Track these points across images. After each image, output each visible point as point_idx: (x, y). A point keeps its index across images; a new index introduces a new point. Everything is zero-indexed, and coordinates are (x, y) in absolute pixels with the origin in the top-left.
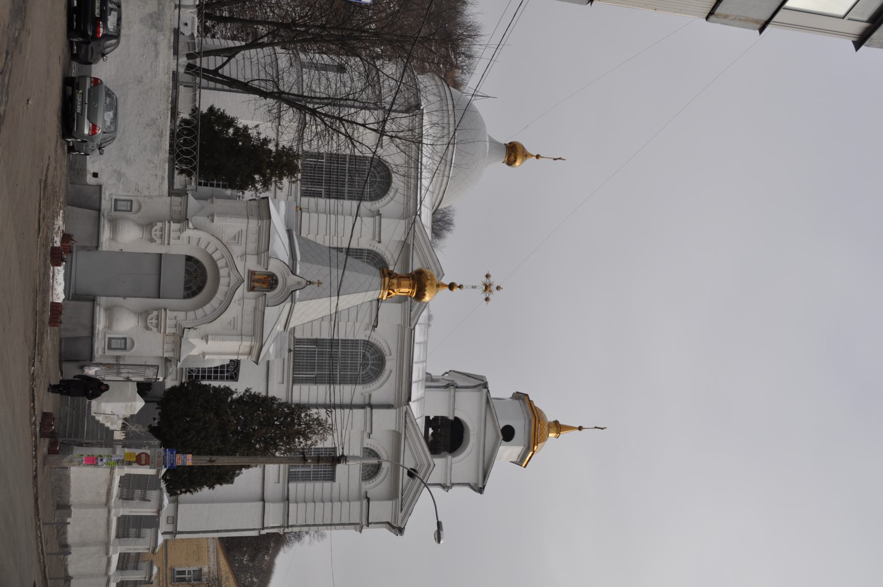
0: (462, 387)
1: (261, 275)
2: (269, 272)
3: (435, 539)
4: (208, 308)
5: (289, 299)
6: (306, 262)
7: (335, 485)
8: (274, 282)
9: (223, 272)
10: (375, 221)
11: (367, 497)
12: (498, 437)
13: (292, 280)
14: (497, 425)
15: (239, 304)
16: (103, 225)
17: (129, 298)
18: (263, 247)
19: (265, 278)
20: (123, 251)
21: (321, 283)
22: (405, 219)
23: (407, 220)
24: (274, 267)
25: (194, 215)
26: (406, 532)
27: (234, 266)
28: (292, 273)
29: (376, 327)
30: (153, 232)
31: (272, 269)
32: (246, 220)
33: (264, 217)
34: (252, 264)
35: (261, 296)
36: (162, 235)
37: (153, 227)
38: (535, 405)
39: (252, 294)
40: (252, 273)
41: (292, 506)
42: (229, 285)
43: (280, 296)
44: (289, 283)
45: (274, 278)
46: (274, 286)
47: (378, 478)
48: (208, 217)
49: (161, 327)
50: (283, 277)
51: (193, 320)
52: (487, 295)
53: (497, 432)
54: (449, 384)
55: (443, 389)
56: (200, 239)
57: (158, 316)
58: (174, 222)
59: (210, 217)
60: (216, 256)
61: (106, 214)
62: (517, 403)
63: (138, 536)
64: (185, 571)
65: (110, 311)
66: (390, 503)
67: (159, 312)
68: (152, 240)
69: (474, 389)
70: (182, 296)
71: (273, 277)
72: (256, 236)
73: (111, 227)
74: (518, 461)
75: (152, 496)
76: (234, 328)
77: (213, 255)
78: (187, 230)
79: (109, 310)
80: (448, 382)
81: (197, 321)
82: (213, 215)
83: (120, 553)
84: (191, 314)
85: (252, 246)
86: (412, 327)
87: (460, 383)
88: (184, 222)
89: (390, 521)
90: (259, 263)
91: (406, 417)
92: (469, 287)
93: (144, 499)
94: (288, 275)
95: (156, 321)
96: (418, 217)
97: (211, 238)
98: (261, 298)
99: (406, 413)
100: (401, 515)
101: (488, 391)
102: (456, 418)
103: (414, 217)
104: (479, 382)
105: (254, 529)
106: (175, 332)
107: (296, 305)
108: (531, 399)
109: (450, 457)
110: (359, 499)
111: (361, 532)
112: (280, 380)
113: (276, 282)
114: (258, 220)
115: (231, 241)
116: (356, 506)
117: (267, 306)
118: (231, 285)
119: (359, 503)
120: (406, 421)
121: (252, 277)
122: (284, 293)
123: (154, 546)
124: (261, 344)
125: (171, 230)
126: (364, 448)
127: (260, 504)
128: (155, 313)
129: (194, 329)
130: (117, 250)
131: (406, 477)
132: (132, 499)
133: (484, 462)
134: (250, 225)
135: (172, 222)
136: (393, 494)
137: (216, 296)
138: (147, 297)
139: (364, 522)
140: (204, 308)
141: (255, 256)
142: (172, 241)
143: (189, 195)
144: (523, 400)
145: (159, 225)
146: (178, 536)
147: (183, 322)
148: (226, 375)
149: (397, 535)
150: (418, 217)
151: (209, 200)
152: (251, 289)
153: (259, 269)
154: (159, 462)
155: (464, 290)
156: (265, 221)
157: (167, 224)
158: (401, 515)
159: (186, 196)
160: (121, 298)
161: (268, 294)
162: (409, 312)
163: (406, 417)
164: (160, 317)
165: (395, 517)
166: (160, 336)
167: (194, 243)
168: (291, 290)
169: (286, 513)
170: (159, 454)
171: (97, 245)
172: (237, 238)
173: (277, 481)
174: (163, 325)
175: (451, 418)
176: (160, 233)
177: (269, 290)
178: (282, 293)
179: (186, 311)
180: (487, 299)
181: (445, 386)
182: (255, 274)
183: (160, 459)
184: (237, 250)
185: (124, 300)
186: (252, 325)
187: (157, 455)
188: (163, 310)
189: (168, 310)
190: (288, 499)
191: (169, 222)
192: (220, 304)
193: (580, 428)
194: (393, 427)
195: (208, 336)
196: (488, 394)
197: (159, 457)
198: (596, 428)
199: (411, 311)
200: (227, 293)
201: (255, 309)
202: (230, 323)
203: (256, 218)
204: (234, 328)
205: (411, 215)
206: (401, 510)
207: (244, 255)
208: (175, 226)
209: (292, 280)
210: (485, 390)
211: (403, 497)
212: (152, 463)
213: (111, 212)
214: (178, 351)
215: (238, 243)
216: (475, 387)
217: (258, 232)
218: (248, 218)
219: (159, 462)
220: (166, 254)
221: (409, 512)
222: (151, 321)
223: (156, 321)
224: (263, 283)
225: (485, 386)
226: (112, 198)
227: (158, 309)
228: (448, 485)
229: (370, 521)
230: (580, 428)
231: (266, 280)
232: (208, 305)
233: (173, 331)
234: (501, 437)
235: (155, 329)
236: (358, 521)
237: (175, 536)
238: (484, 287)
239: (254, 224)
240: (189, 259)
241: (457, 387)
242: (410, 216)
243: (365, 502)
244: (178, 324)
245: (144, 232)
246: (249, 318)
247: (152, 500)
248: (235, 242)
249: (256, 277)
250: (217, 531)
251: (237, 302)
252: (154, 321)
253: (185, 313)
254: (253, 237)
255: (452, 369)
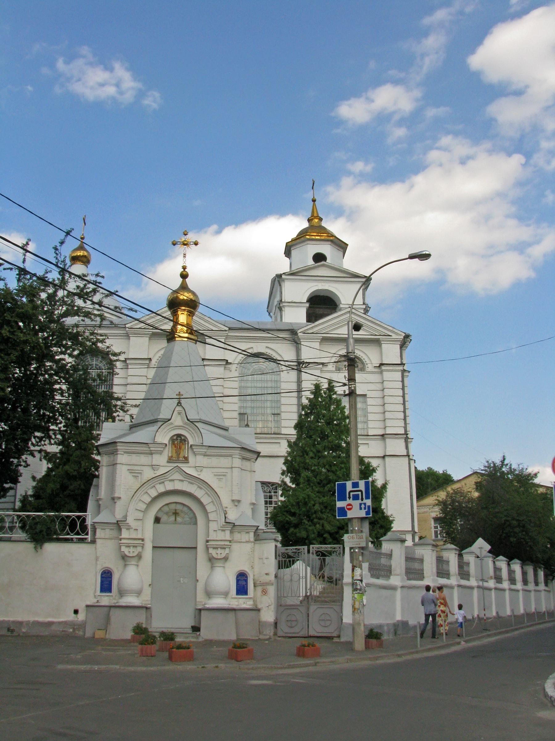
0: (281, 296)
1: (172, 452)
2: (169, 443)
3: (427, 259)
4: (205, 500)
5: (196, 424)
6: (160, 410)
7: (369, 394)
8: (179, 439)
9: (170, 486)
10: (131, 364)
11: (379, 366)
12: (323, 265)
13: (177, 420)
14: (313, 266)
15: (201, 471)
16: (124, 603)
17: (198, 576)
18: (144, 449)
19: (175, 447)
20: (150, 583)
21: (179, 392)
22: (129, 337)
23: (130, 335)
24: (164, 437)
25: (114, 516)
26: (408, 332)
27: (163, 475)
28: (169, 420)
29: (227, 361)
30: (131, 555)
31: (166, 440)
32: (118, 466)
33: (115, 448)
34: (161, 459)
35: (192, 449)
36: (134, 546)
37: (126, 556)
38: (295, 236)
39: (191, 459)
40: (170, 460)
41: (389, 431)
42: (182, 481)
43: (193, 431)
44: (181, 424)
45: (175, 438)
46: (183, 438)
47: (362, 357)
48: (115, 503)
49: (224, 545)
50: (174, 429)
51: (217, 514)
52: (192, 243)
53: (319, 266)
54: (278, 308)
55: (283, 312)
56: (136, 509)
57: (214, 548)
58: (121, 535)
59: (116, 501)
60: (154, 493)
61: (116, 602)
62: (294, 253)
63: (421, 561)
64: (435, 531)
65: (209, 594)
66: (383, 346)
67: (210, 547)
68: (139, 557)
69: (283, 286)
70: (194, 526)
71: (174, 440)
72: (134, 455)
73: (127, 596)
74: (342, 250)
75: (388, 548)
76: (224, 475)
77: (153, 497)
78: (127, 522)
79: (209, 594)
80: (277, 308)
81: (218, 511)
82: (113, 499)
83: (437, 577)
84: (212, 516)
85: (144, 459)
86: (227, 329)
87: (278, 299)
88: (120, 525)
89: (398, 346)
90: (160, 453)
91: (308, 333)
92: (184, 260)
93: (390, 556)
94: (172, 424)
95: (219, 549)
96: (127, 326)
97: (135, 498)
98: (194, 450)
99: (304, 333)
100: (394, 336)
101: (284, 273)
102: (307, 301)
103: (127, 329)
104: (276, 282)
105: (409, 464)
106: (229, 531)
107: (201, 418)
108: (290, 240)
109: (341, 306)
110: (381, 373)
111: (409, 372)
112: (277, 445)
113: (179, 436)
114: (117, 454)
115: (139, 480)
116: (387, 375)
117: (202, 443)
118: (182, 478)
119: (384, 373)
120: (312, 333)
121: (174, 459)
122: (189, 428)
123: (431, 546)
124: (239, 449)
125: (128, 537)
126: (336, 370)
127: (387, 459)
128: (211, 550)
129: (227, 513)
130: (150, 589)
131: (361, 332)
132: (390, 566)
133: (344, 277)
134: (124, 461)
135: (120, 537)
136: (376, 342)
137: (193, 493)
138: (196, 559)
139: (401, 368)
140: (205, 503)
141: (153, 457)
142: (140, 536)
143: (96, 520)
144: (291, 247)
145: (123, 549)
146: (416, 530)
147: (219, 524)
148: (273, 494)
149: (411, 340)
150: (127, 326)
151: (100, 502)
152: (186, 460)
153: (167, 452)
154: (358, 537)
155: (187, 265)
156: (118, 448)
157: (123, 541)
158: (394, 336)
159: (95, 525)
160: (198, 584)
161: (191, 442)
162: (213, 332)
163: (308, 333)
164: (215, 546)
165: (395, 341)
166: (235, 546)
167: (140, 515)
168: (186, 421)
169: (394, 436)
170: (350, 537)
171: (145, 609)
172: (135, 474)
173: (366, 446)
174: (222, 543)
175: (308, 305)
176: (131, 548)
177: (186, 443)
178: (189, 430)
179: (208, 520)
180: (196, 244)
181: (280, 311)
182: (172, 457)
183: (355, 537)
184: (148, 474)
185: (199, 581)
186: (221, 458)
187: (351, 540)
188: (208, 543)
189: (208, 539)
190: (383, 435)
191: (121, 539)
192: (201, 488)
193: (314, 201)
194: (317, 345)
195: (233, 501)
196: (287, 274)
197: (353, 537)
198: (313, 188)
199: (213, 330)
200: (189, 482)
201: (205, 455)
202: (220, 480)
203: (116, 456)
204: (224, 475)
205: (125, 332)
206: (389, 336)
207: (153, 467)
208: (125, 534)
209: (177, 420)
210: (283, 277)
211: (377, 334)
212: (359, 544)
213: (112, 596)
214: (247, 528)
215: (140, 473)
216: (280, 285)
217: (130, 454)
218: (117, 464)
219: (358, 537)
220: (153, 542)
221: (391, 328)
222: (219, 554)
223: (219, 549)
224: (180, 448)
225: (279, 276)
226: (99, 595)
227: (207, 548)
228: (364, 307)
229: (400, 363)
230: (314, 201)
231: (176, 445)
232: (202, 500)
233: (228, 533)
234: (323, 263)
235: (227, 551)
236: (400, 374)
237: (416, 532)
238: (185, 246)
239: (121, 458)
240: (157, 520)
241: (281, 301)
242: (127, 333)
243: (383, 368)
244: (221, 528)
245: (130, 563)
246: (214, 461)
247: (391, 548)
248: (140, 478)
249: (175, 455)
250: (411, 496)
251: (199, 473)
252: (219, 551)
253: (210, 522)
254: (135, 459)
255: (266, 310)
